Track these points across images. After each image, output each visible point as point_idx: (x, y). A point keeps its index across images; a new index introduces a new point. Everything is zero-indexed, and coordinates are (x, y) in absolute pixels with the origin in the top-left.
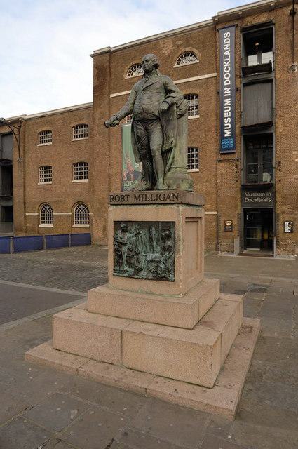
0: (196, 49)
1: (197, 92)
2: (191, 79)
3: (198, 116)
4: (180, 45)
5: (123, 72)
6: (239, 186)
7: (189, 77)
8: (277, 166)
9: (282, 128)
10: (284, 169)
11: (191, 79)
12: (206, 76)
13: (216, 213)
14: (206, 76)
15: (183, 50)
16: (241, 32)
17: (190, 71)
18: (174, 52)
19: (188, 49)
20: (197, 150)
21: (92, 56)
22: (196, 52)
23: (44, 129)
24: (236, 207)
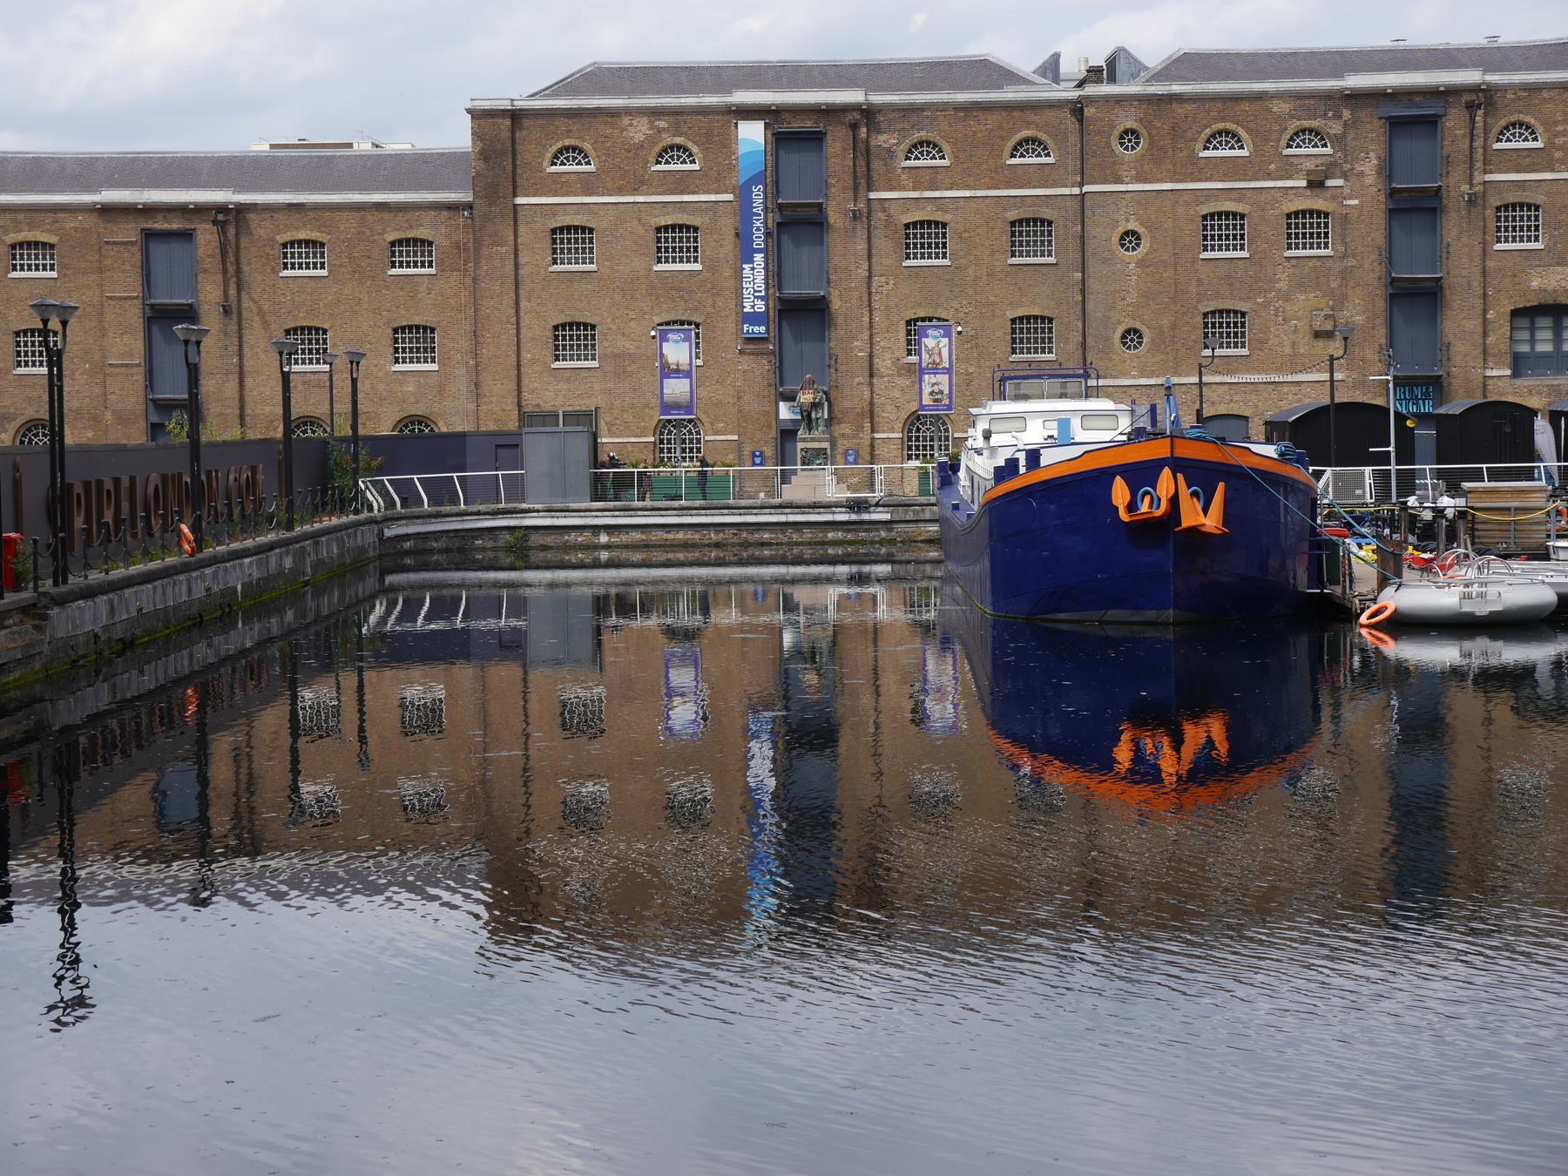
0: (695, 143)
1: (696, 223)
2: (686, 198)
3: (697, 267)
4: (664, 129)
5: (542, 156)
6: (773, 392)
7: (682, 192)
8: (833, 362)
9: (839, 303)
10: (841, 368)
11: (686, 198)
12: (713, 198)
13: (735, 437)
14: (713, 198)
15: (668, 140)
16: (773, 134)
17: (682, 183)
18: (652, 141)
19: (679, 140)
20: (697, 326)
21: (469, 111)
22: (695, 149)
23: (302, 236)
24: (769, 427)
